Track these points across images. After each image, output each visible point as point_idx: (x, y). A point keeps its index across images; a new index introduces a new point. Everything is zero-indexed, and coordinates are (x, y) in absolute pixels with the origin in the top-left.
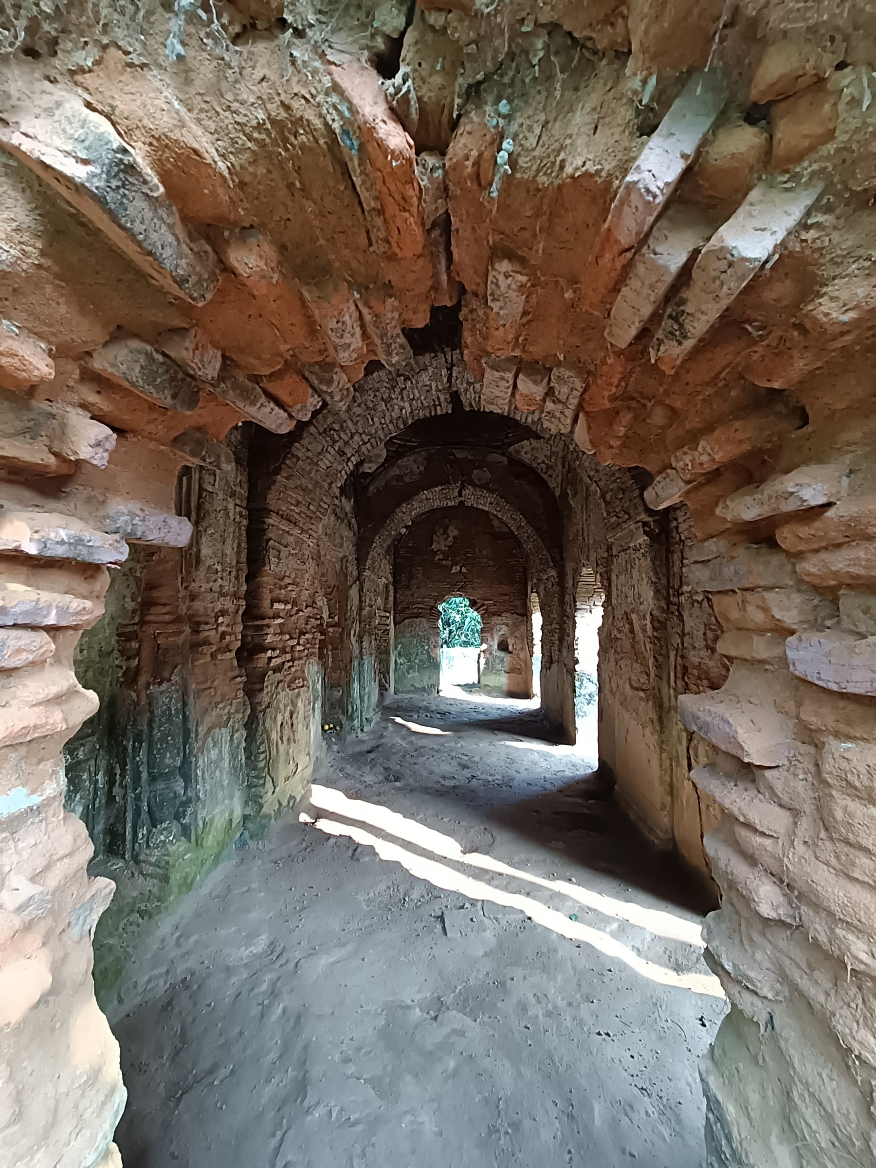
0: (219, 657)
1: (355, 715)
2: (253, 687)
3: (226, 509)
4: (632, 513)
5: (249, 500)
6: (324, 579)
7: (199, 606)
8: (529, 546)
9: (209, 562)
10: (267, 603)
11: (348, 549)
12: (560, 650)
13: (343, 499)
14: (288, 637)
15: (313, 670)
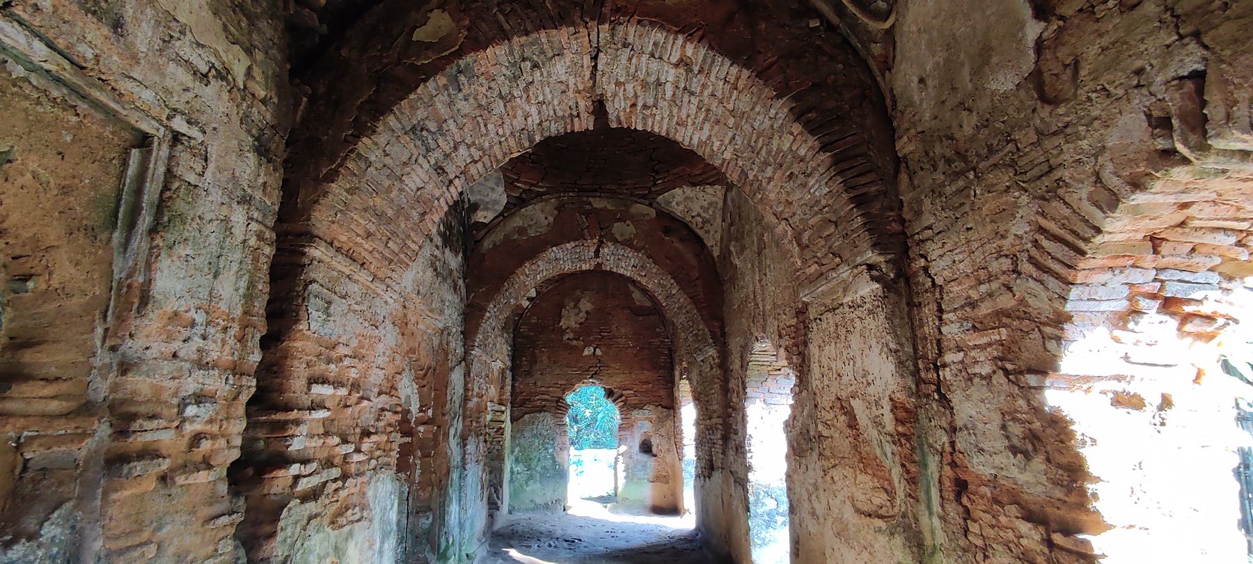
0: (180, 480)
1: (451, 551)
2: (256, 530)
3: (226, 220)
4: (846, 255)
5: (282, 217)
6: (414, 357)
7: (139, 384)
8: (680, 320)
9: (171, 306)
10: (297, 385)
11: (451, 317)
12: (724, 453)
13: (447, 250)
14: (337, 440)
15: (383, 496)
